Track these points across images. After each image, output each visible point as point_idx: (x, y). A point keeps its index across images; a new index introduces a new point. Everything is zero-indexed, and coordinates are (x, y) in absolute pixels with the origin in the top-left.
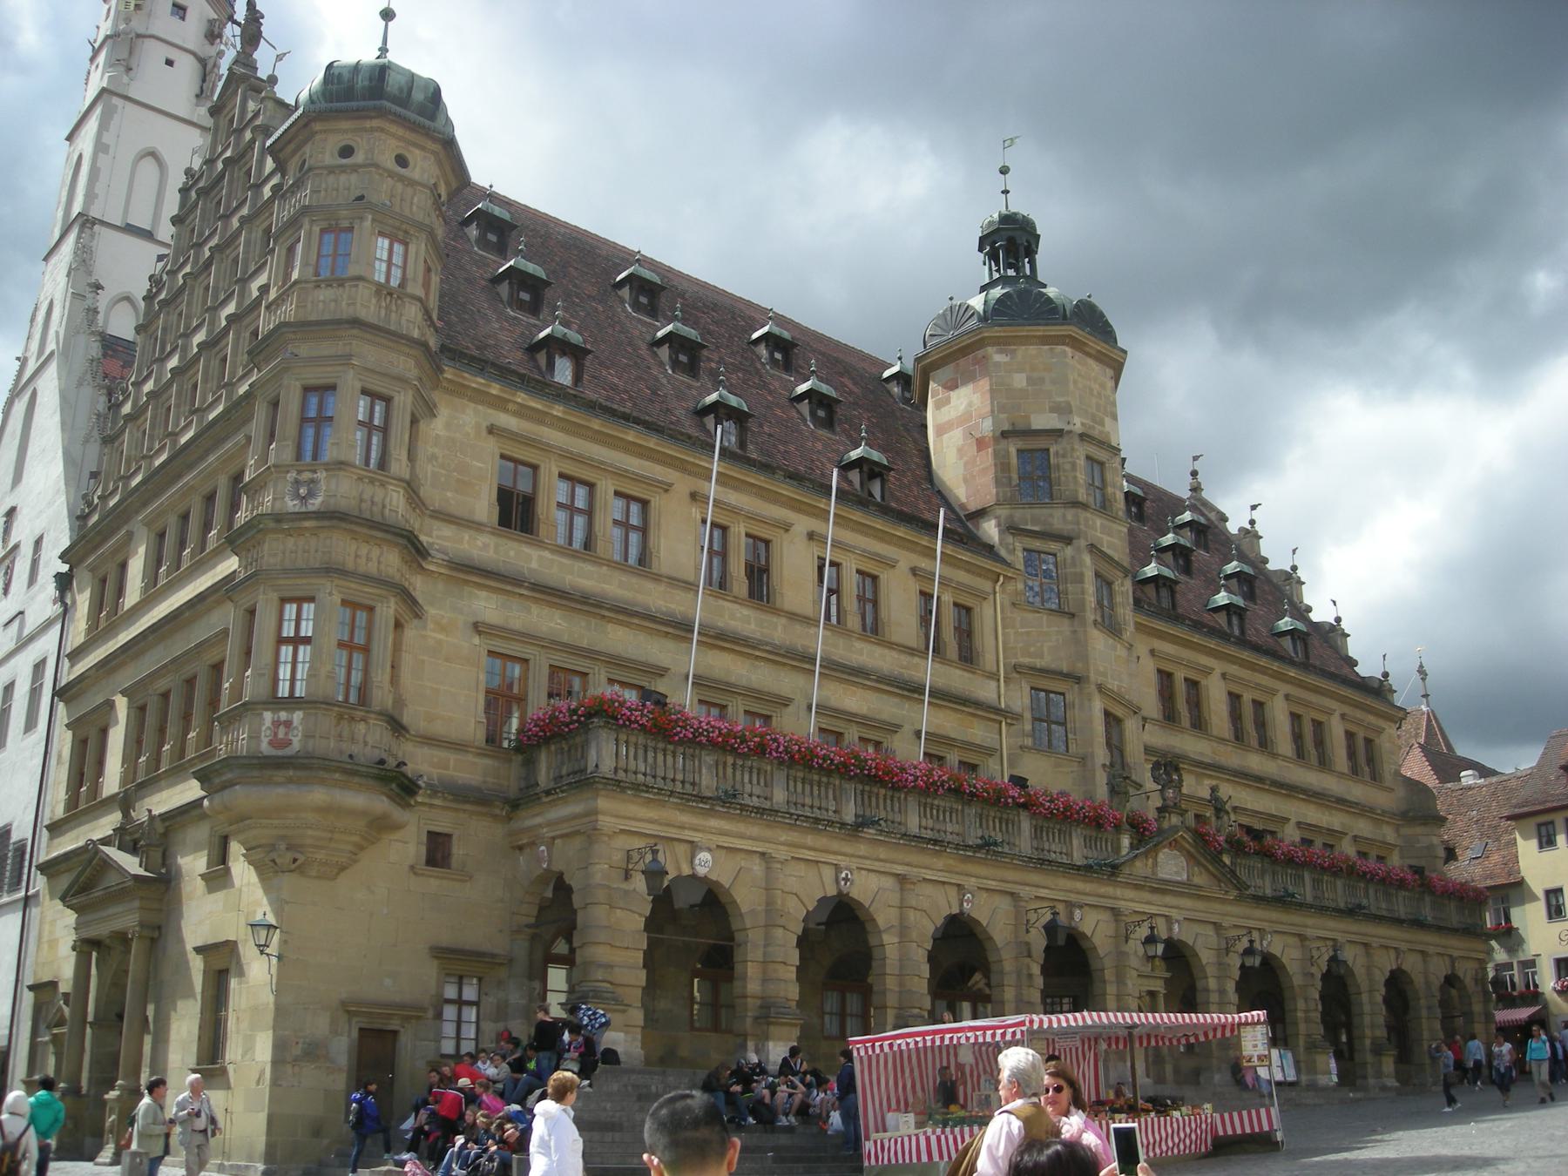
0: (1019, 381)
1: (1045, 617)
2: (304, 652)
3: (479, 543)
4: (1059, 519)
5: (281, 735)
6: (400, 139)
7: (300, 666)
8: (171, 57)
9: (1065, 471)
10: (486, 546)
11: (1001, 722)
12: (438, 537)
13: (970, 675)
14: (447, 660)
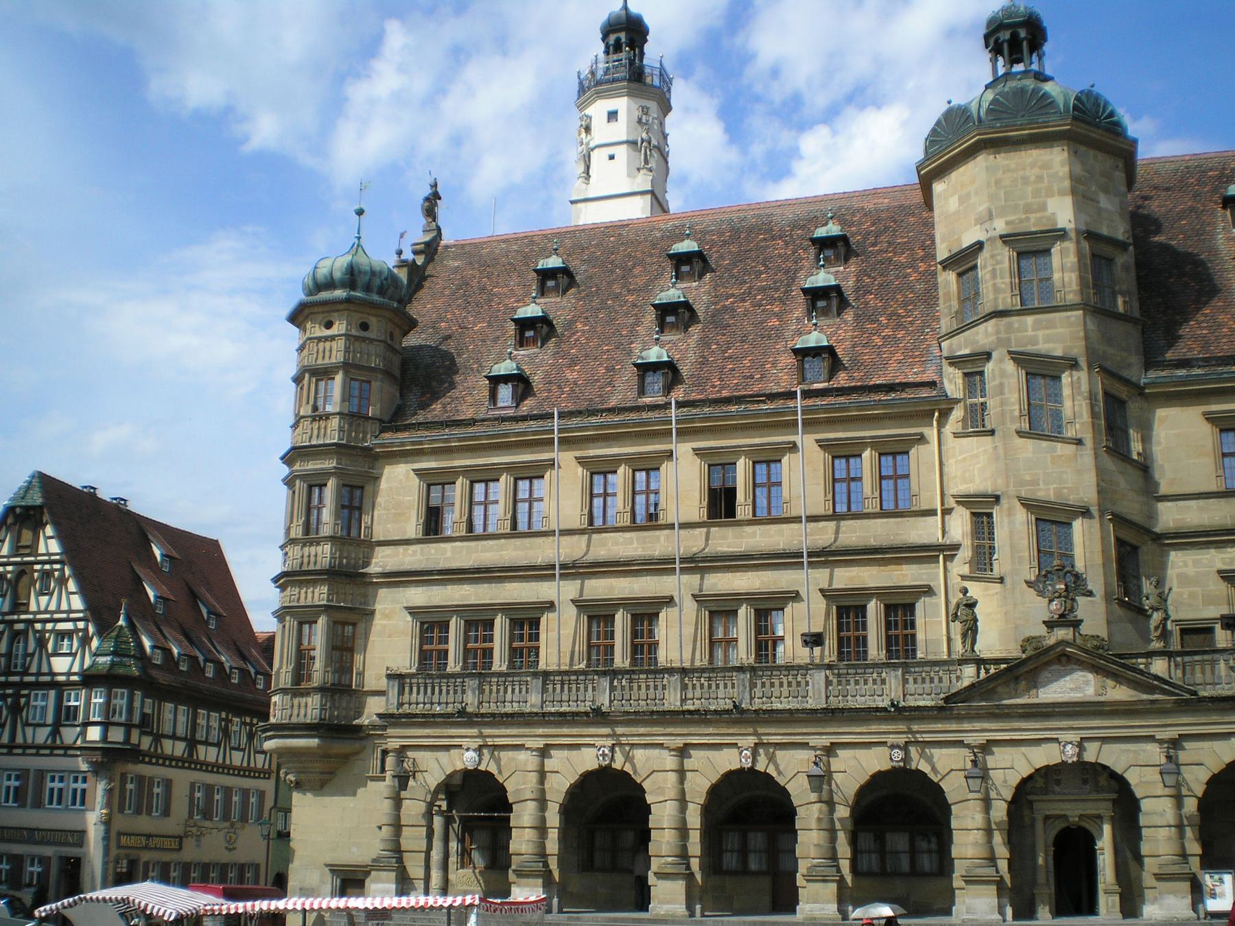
3: (410, 552)
4: (984, 336)
6: (323, 312)
8: (611, 153)
10: (415, 552)
11: (938, 556)
12: (382, 557)
13: (900, 519)
14: (390, 636)
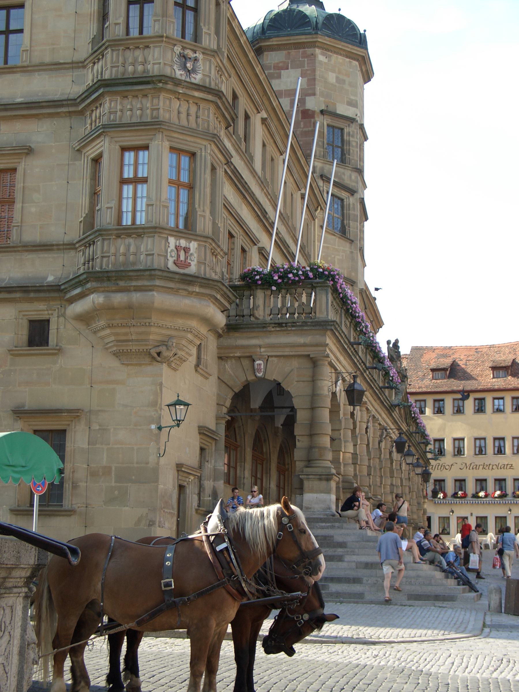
0: (332, 78)
1: (337, 239)
2: (142, 189)
5: (182, 258)
7: (139, 201)
9: (353, 146)
